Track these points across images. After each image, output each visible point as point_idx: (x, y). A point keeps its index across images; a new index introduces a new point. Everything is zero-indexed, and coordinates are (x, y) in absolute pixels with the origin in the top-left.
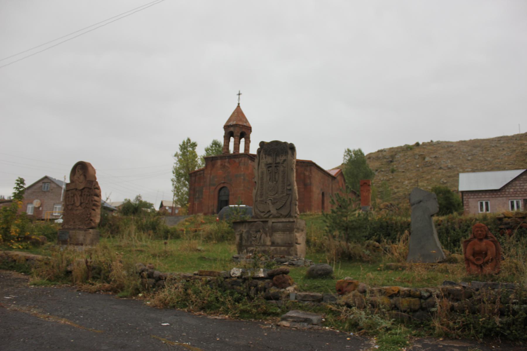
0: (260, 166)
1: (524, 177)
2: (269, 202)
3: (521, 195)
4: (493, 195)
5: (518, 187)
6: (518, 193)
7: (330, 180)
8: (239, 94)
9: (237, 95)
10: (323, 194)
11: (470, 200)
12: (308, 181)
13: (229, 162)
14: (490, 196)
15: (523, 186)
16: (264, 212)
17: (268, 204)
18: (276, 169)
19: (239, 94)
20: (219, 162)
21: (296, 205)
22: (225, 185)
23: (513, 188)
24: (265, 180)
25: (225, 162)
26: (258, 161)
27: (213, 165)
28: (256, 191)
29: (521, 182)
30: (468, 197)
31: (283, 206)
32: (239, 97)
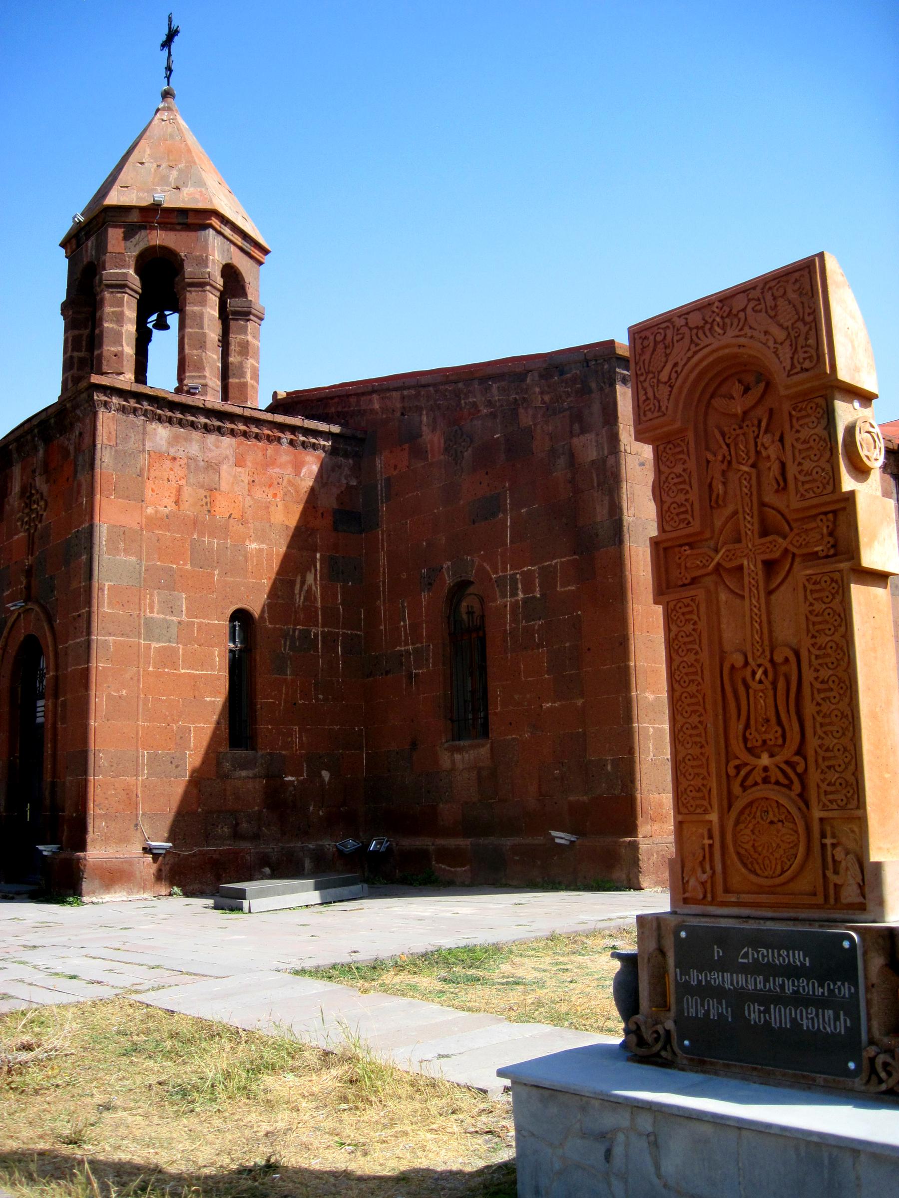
12: (601, 512)
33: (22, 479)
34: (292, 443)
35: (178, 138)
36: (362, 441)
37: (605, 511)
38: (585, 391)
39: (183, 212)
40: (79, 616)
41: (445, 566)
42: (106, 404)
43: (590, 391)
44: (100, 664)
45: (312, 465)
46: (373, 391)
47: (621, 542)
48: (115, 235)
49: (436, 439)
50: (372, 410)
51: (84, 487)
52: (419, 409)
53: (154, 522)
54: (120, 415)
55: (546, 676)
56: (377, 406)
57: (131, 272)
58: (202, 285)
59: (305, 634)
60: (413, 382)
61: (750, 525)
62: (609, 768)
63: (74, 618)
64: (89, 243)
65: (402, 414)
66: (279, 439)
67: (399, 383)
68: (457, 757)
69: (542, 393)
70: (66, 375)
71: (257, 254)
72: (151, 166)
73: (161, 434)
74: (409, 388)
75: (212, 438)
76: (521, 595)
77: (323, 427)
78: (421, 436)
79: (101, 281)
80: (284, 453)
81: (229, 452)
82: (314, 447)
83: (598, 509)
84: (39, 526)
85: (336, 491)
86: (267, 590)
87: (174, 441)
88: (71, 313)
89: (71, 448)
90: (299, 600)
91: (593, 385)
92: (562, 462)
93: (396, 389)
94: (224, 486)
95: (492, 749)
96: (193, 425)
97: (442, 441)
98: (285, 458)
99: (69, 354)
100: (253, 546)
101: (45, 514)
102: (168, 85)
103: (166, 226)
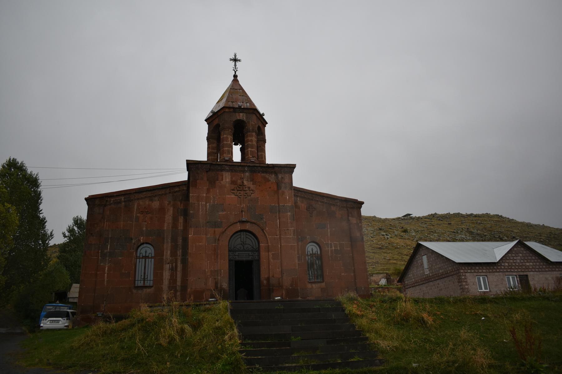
1: (515, 249)
3: (516, 270)
4: (490, 269)
5: (512, 261)
6: (513, 268)
11: (467, 274)
12: (358, 234)
13: (252, 180)
14: (487, 271)
15: (516, 259)
22: (248, 227)
23: (508, 261)
27: (213, 182)
29: (513, 255)
30: (465, 271)
32: (235, 65)
33: (231, 178)
40: (288, 230)
41: (307, 237)
55: (342, 268)
62: (363, 289)
63: (284, 230)
64: (241, 114)
68: (314, 285)
76: (333, 248)
95: (326, 284)
97: (305, 207)
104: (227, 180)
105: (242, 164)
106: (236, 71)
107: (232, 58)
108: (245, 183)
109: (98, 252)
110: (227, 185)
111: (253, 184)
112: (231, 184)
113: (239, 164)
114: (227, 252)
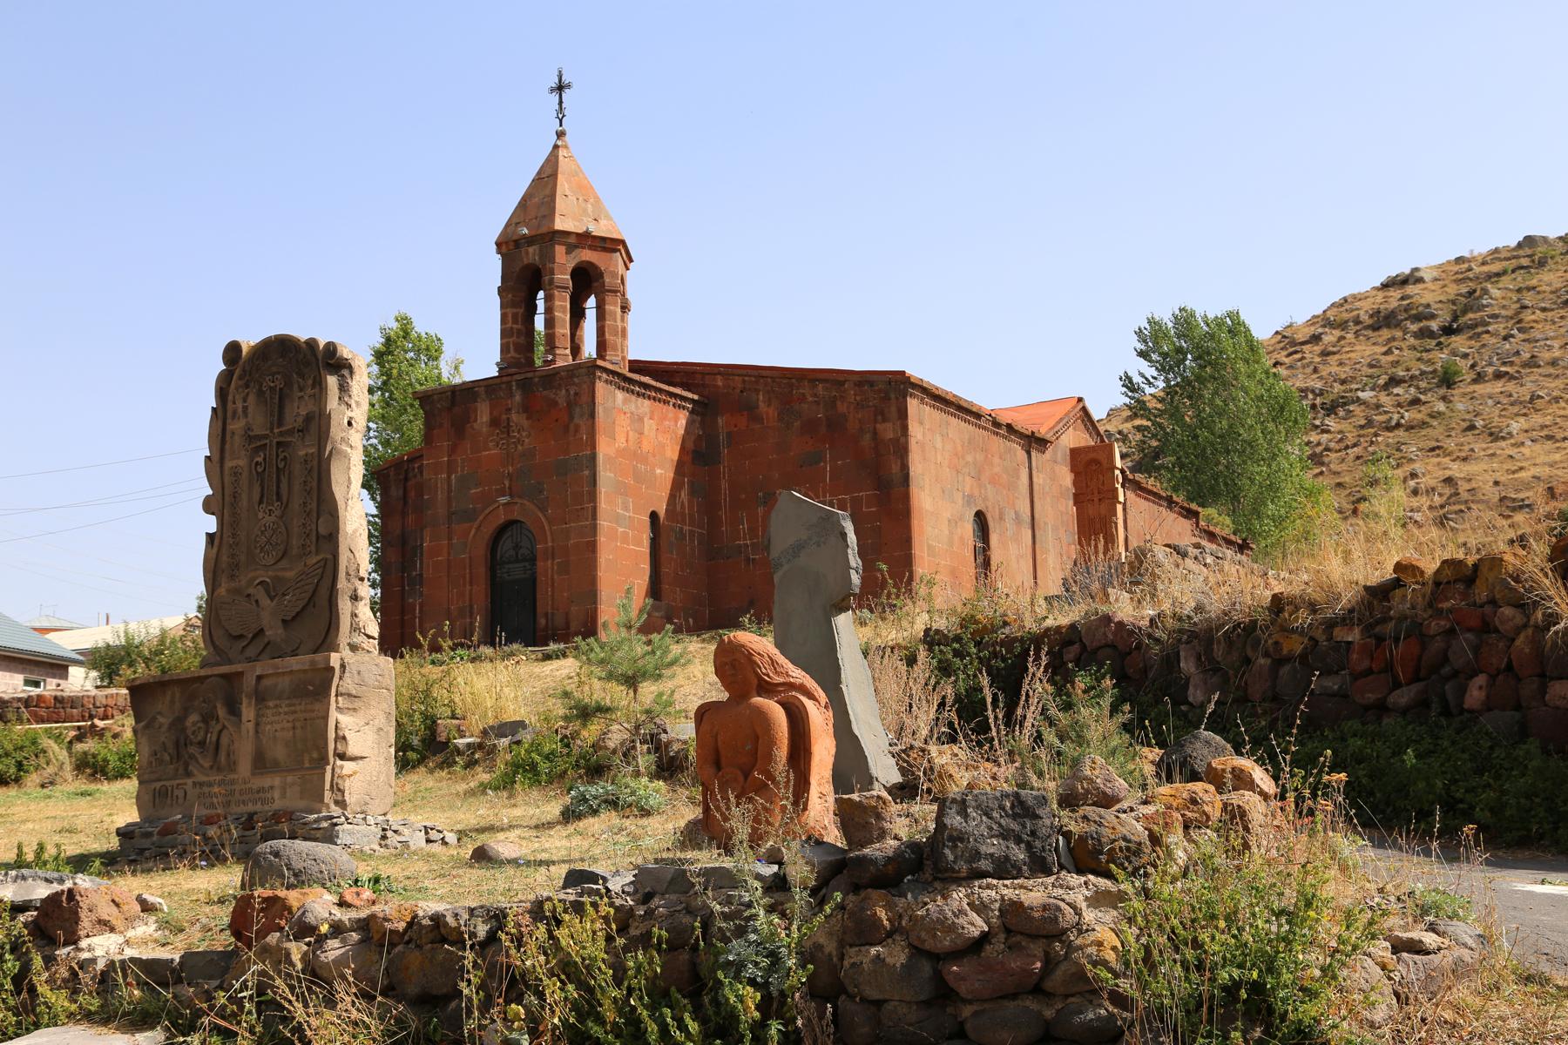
0: (227, 446)
2: (260, 594)
7: (1021, 454)
8: (560, 88)
9: (552, 90)
10: (981, 519)
13: (526, 409)
16: (241, 636)
17: (257, 601)
18: (281, 456)
19: (560, 88)
20: (483, 414)
21: (355, 598)
24: (244, 503)
25: (509, 410)
26: (220, 423)
27: (461, 425)
28: (215, 550)
31: (304, 608)
32: (561, 103)
33: (491, 413)
34: (674, 405)
35: (581, 175)
36: (706, 404)
37: (899, 468)
38: (887, 398)
39: (604, 239)
42: (600, 378)
43: (889, 399)
44: (602, 539)
45: (679, 421)
46: (719, 373)
47: (908, 486)
48: (560, 250)
49: (771, 411)
50: (716, 387)
51: (583, 429)
52: (757, 391)
53: (621, 453)
54: (605, 385)
56: (720, 383)
57: (569, 277)
58: (616, 292)
59: (681, 529)
60: (756, 373)
61: (1096, 492)
63: (577, 510)
64: (531, 250)
65: (742, 392)
66: (669, 402)
67: (744, 372)
69: (855, 395)
70: (505, 341)
71: (627, 262)
72: (572, 198)
73: (620, 395)
74: (750, 376)
75: (640, 400)
77: (690, 395)
78: (757, 407)
79: (551, 281)
80: (669, 410)
81: (647, 410)
82: (684, 408)
83: (893, 466)
84: (520, 447)
85: (693, 438)
86: (666, 500)
87: (625, 401)
88: (510, 296)
89: (562, 402)
90: (678, 508)
91: (893, 396)
92: (868, 437)
93: (738, 375)
94: (646, 432)
96: (633, 392)
98: (671, 415)
99: (509, 325)
100: (658, 471)
101: (527, 440)
102: (561, 125)
103: (591, 248)
104: (485, 419)
105: (505, 379)
106: (564, 116)
107: (554, 85)
108: (514, 417)
109: (403, 577)
110: (484, 430)
111: (528, 419)
112: (490, 426)
113: (498, 381)
114: (482, 571)
